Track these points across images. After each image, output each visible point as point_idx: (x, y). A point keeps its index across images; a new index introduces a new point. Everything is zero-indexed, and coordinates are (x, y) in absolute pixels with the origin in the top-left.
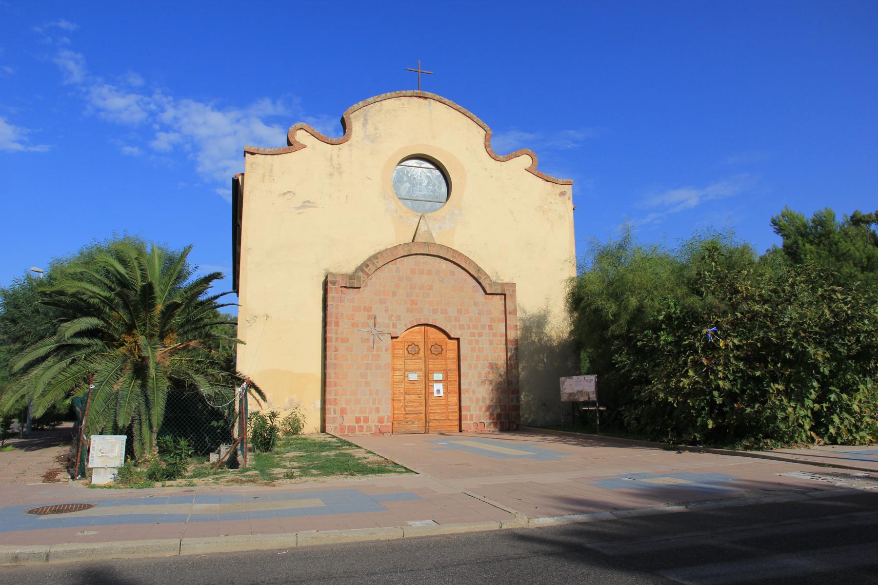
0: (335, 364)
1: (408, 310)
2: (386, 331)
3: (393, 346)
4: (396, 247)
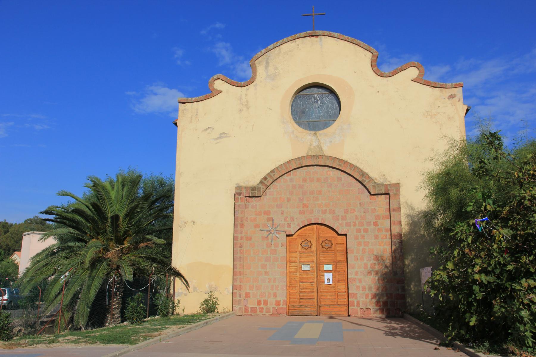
0: (240, 257)
1: (300, 212)
2: (282, 229)
3: (290, 243)
4: (289, 162)
